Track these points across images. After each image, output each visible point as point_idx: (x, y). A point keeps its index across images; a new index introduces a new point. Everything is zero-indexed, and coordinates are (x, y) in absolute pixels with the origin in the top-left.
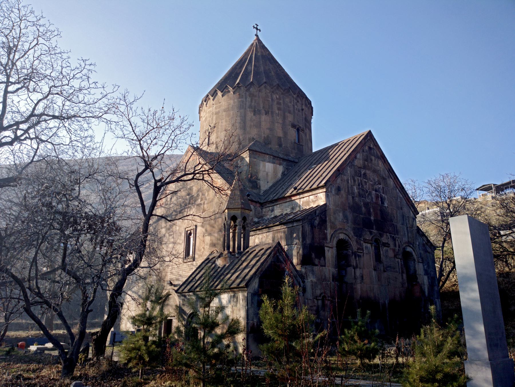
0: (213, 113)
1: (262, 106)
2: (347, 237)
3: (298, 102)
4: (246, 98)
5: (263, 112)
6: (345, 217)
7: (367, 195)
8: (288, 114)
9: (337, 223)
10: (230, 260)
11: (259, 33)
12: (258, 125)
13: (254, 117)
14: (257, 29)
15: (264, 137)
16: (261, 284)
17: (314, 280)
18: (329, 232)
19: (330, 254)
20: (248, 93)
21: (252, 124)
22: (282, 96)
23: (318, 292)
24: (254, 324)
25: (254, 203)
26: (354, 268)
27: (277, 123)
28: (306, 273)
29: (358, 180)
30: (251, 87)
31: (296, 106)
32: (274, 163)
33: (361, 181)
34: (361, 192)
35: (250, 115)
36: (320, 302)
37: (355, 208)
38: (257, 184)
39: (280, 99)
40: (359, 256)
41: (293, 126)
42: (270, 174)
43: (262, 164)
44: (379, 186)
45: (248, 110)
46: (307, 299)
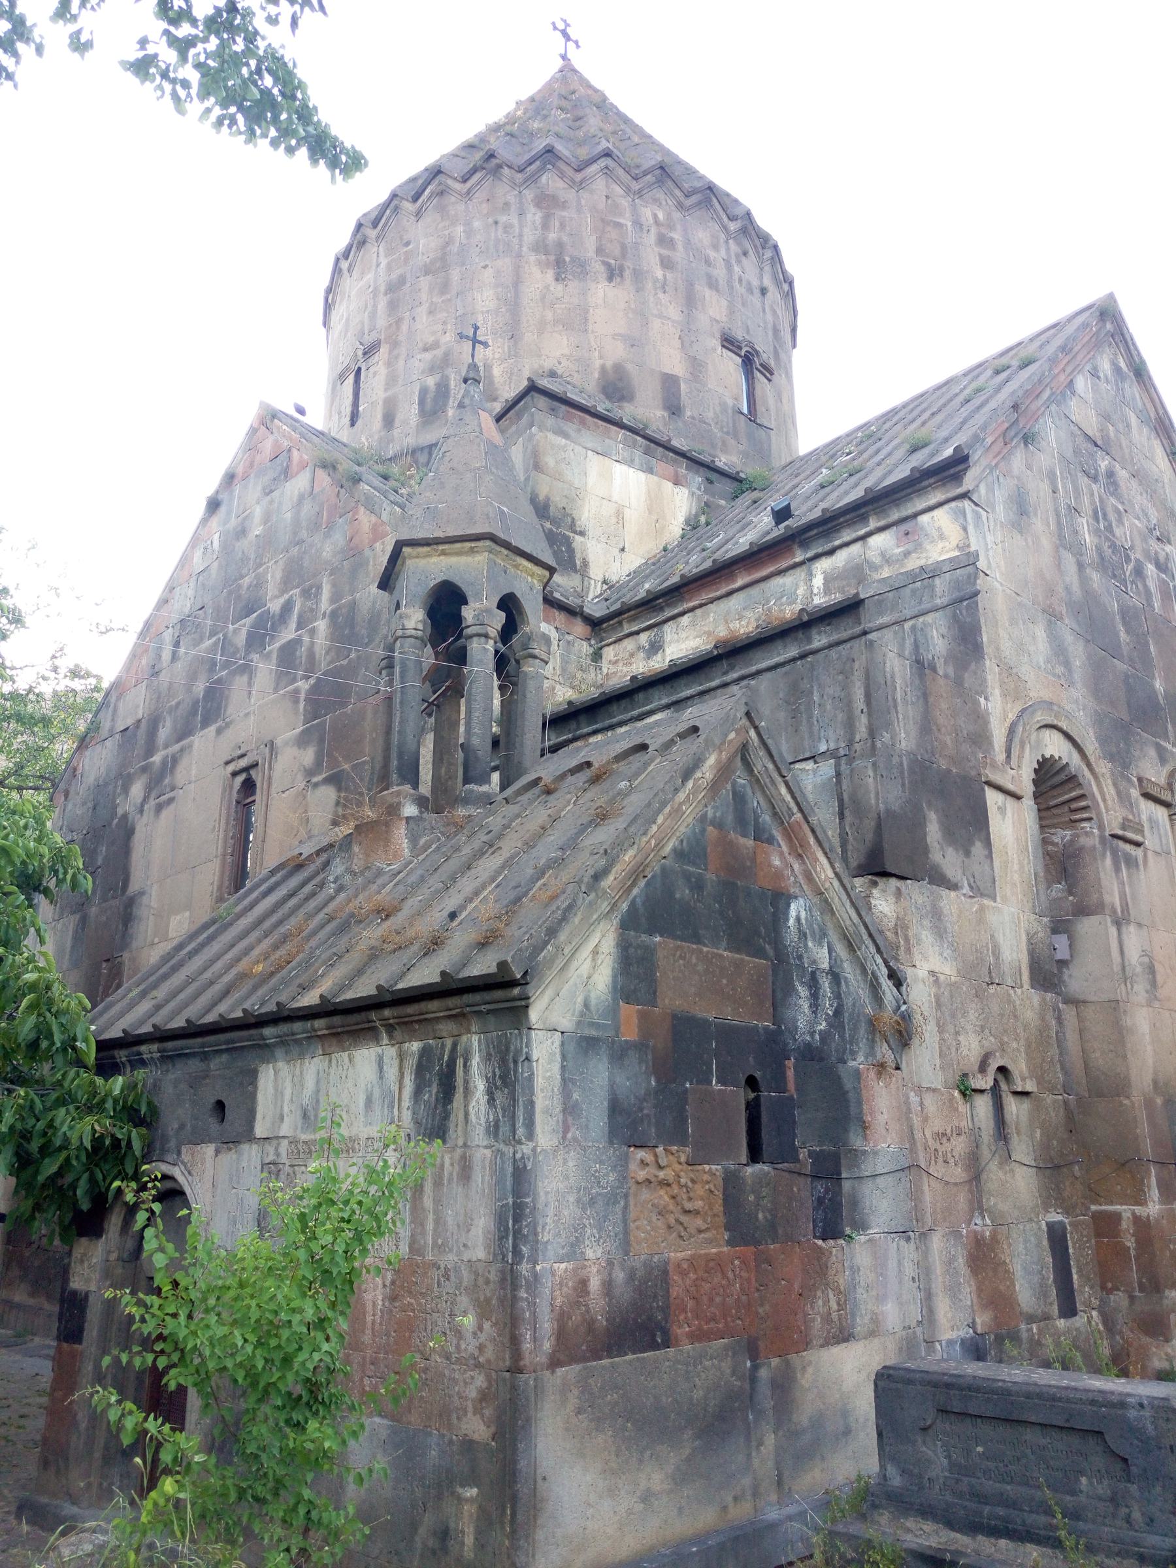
0: (375, 293)
1: (591, 244)
2: (1076, 756)
3: (745, 254)
4: (521, 214)
5: (598, 267)
6: (1059, 652)
7: (1129, 569)
8: (708, 293)
9: (1026, 671)
10: (413, 839)
11: (572, 53)
12: (577, 321)
13: (557, 289)
14: (567, 38)
15: (603, 369)
16: (635, 974)
17: (948, 970)
18: (998, 710)
19: (1012, 826)
20: (529, 195)
21: (549, 315)
22: (677, 215)
23: (971, 1047)
24: (584, 1283)
25: (560, 617)
26: (1118, 924)
27: (660, 316)
28: (901, 926)
29: (1092, 495)
30: (542, 169)
31: (737, 269)
32: (650, 470)
33: (1101, 500)
34: (1108, 552)
35: (538, 278)
36: (983, 1104)
37: (1092, 622)
38: (571, 551)
39: (672, 227)
40: (1131, 862)
41: (729, 343)
42: (635, 515)
43: (595, 464)
44: (1168, 548)
45: (532, 259)
46: (919, 1090)
